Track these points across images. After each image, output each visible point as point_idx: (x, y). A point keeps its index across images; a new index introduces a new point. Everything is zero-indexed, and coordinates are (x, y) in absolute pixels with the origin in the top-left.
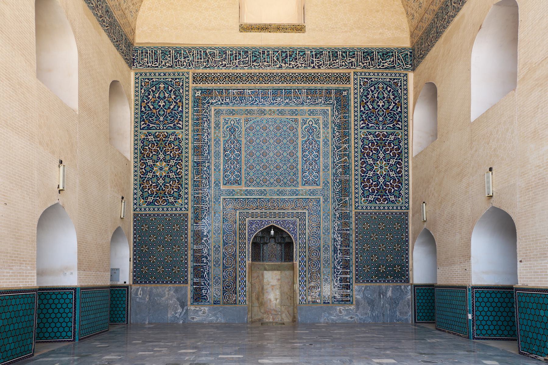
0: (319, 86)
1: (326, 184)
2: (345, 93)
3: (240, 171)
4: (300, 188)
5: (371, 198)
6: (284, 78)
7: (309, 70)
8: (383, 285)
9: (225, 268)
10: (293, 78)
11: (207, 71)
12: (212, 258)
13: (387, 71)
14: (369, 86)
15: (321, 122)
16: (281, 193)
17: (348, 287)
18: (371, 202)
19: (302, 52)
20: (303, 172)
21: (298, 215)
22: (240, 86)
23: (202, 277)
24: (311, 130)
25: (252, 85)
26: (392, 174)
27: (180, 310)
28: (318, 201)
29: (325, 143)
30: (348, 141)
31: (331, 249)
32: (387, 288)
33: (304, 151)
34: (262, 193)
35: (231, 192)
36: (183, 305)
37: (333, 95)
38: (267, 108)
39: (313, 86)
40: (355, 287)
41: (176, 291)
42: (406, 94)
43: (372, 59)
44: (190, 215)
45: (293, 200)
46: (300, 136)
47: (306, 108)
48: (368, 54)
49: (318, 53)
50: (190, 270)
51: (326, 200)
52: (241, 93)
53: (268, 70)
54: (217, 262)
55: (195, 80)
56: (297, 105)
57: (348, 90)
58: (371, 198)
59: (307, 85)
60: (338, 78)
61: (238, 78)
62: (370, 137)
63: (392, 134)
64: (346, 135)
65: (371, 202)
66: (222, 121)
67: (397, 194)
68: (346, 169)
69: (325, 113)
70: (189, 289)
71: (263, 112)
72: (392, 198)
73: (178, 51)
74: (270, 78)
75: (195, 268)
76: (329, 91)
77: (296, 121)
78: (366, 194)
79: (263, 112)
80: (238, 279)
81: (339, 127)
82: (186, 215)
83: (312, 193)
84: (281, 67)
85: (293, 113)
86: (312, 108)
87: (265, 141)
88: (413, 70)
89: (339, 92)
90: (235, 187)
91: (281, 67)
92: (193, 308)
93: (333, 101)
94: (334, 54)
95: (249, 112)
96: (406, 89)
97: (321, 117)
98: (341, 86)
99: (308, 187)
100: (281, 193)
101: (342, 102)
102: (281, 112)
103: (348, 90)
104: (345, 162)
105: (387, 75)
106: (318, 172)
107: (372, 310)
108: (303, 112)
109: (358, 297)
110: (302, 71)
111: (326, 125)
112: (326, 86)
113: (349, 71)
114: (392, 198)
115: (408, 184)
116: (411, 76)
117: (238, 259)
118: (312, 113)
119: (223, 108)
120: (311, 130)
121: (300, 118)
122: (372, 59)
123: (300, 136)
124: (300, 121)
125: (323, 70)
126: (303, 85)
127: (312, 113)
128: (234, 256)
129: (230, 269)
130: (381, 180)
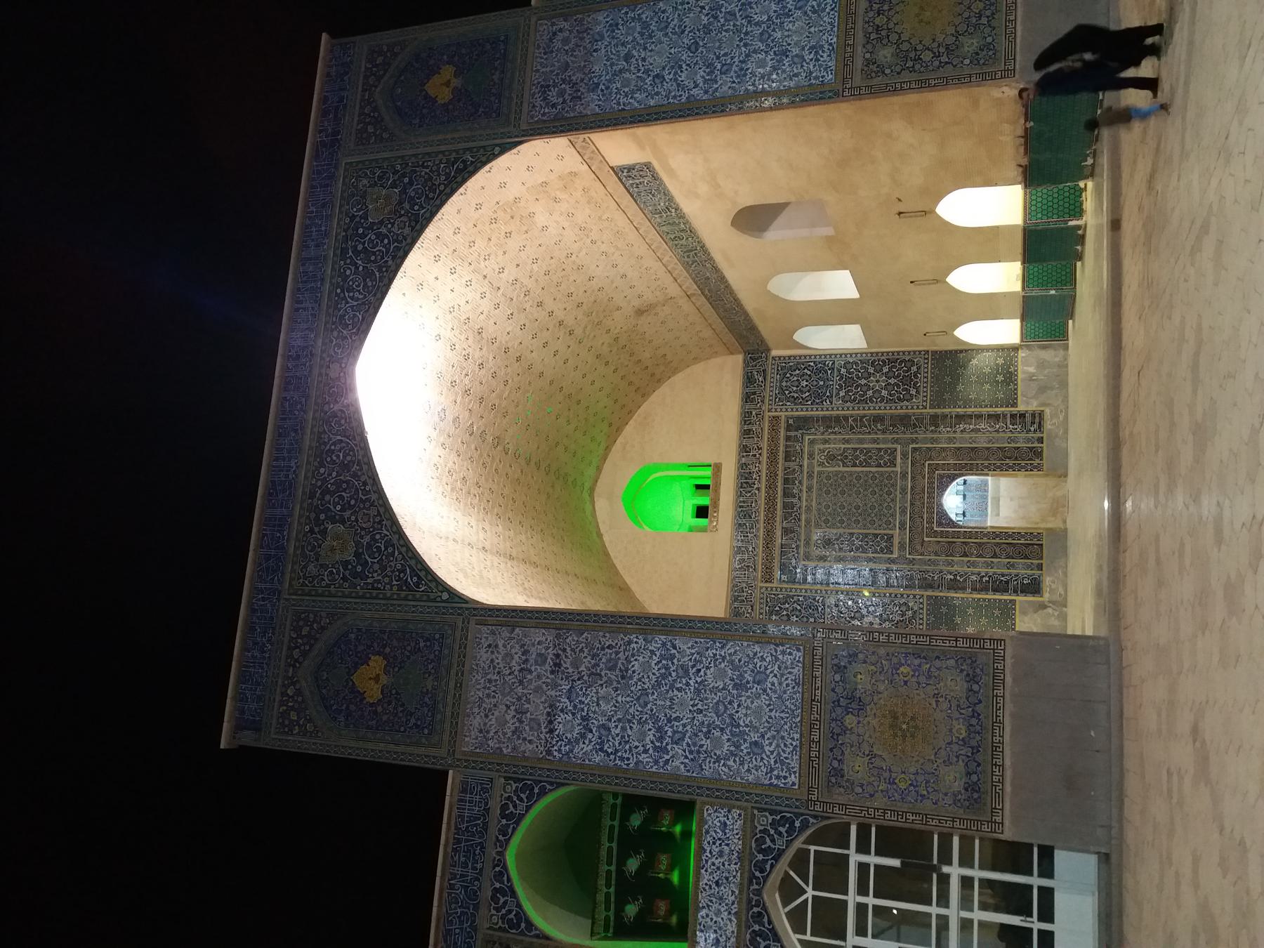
0: (782, 448)
1: (896, 441)
2: (791, 421)
3: (876, 536)
4: (898, 469)
5: (913, 392)
6: (771, 486)
7: (764, 459)
8: (1020, 376)
9: (995, 556)
10: (772, 476)
11: (760, 568)
12: (983, 571)
13: (768, 378)
14: (783, 396)
15: (822, 447)
16: (904, 490)
17: (1023, 416)
18: (918, 392)
19: (742, 466)
20: (879, 466)
21: (932, 472)
22: (778, 533)
23: (1007, 582)
24: (831, 458)
25: (778, 519)
26: (885, 370)
27: (1050, 610)
28: (915, 449)
29: (848, 441)
30: (846, 418)
31: (973, 435)
32: (1024, 372)
33: (854, 465)
34: (903, 512)
35: (902, 547)
36: (1043, 606)
37: (793, 434)
38: (804, 504)
39: (781, 455)
40: (1021, 407)
41: (1024, 613)
42: (795, 357)
43: (754, 393)
44: (930, 593)
45: (913, 478)
46: (836, 469)
47: (806, 463)
48: (747, 398)
49: (744, 449)
50: (998, 596)
51: (913, 441)
52: (786, 531)
53: (762, 502)
54: (990, 565)
55: (769, 581)
56: (802, 472)
57: (788, 418)
58: (913, 392)
59: (781, 461)
60: (774, 428)
61: (769, 534)
62: (842, 394)
63: (839, 371)
64: (837, 419)
65: (918, 392)
66: (818, 552)
67: (909, 364)
68: (878, 419)
69: (812, 442)
70: (1020, 599)
71: (809, 509)
72: (914, 369)
73: (736, 599)
74: (771, 501)
75: (995, 590)
76: (788, 438)
77: (820, 473)
78: (908, 397)
79: (809, 509)
80: (1010, 541)
81: (828, 427)
82: (929, 597)
83: (904, 455)
84: (758, 489)
85: (810, 476)
86: (806, 456)
87: (842, 507)
88: (769, 350)
89: (789, 428)
90: (896, 541)
91: (758, 489)
92: (1047, 596)
93: (799, 433)
94: (746, 433)
95: (808, 522)
96: (789, 357)
97: (817, 447)
98: (783, 425)
99: (899, 460)
100: (904, 490)
101: (802, 424)
102: (810, 489)
103: (788, 418)
104: (869, 421)
105: (773, 377)
106: (880, 449)
107: (1052, 388)
108: (811, 466)
109: (1035, 404)
110: (764, 467)
111: (826, 441)
112: (782, 442)
113: (766, 419)
114: (914, 369)
115: (898, 353)
116: (774, 353)
117: (985, 540)
118: (811, 456)
119: (802, 550)
120: (831, 458)
121: (817, 469)
122: (754, 393)
123: (836, 469)
124: (821, 469)
125: (765, 445)
126: (780, 465)
127: (811, 456)
128: (980, 544)
129: (997, 550)
130: (892, 381)
